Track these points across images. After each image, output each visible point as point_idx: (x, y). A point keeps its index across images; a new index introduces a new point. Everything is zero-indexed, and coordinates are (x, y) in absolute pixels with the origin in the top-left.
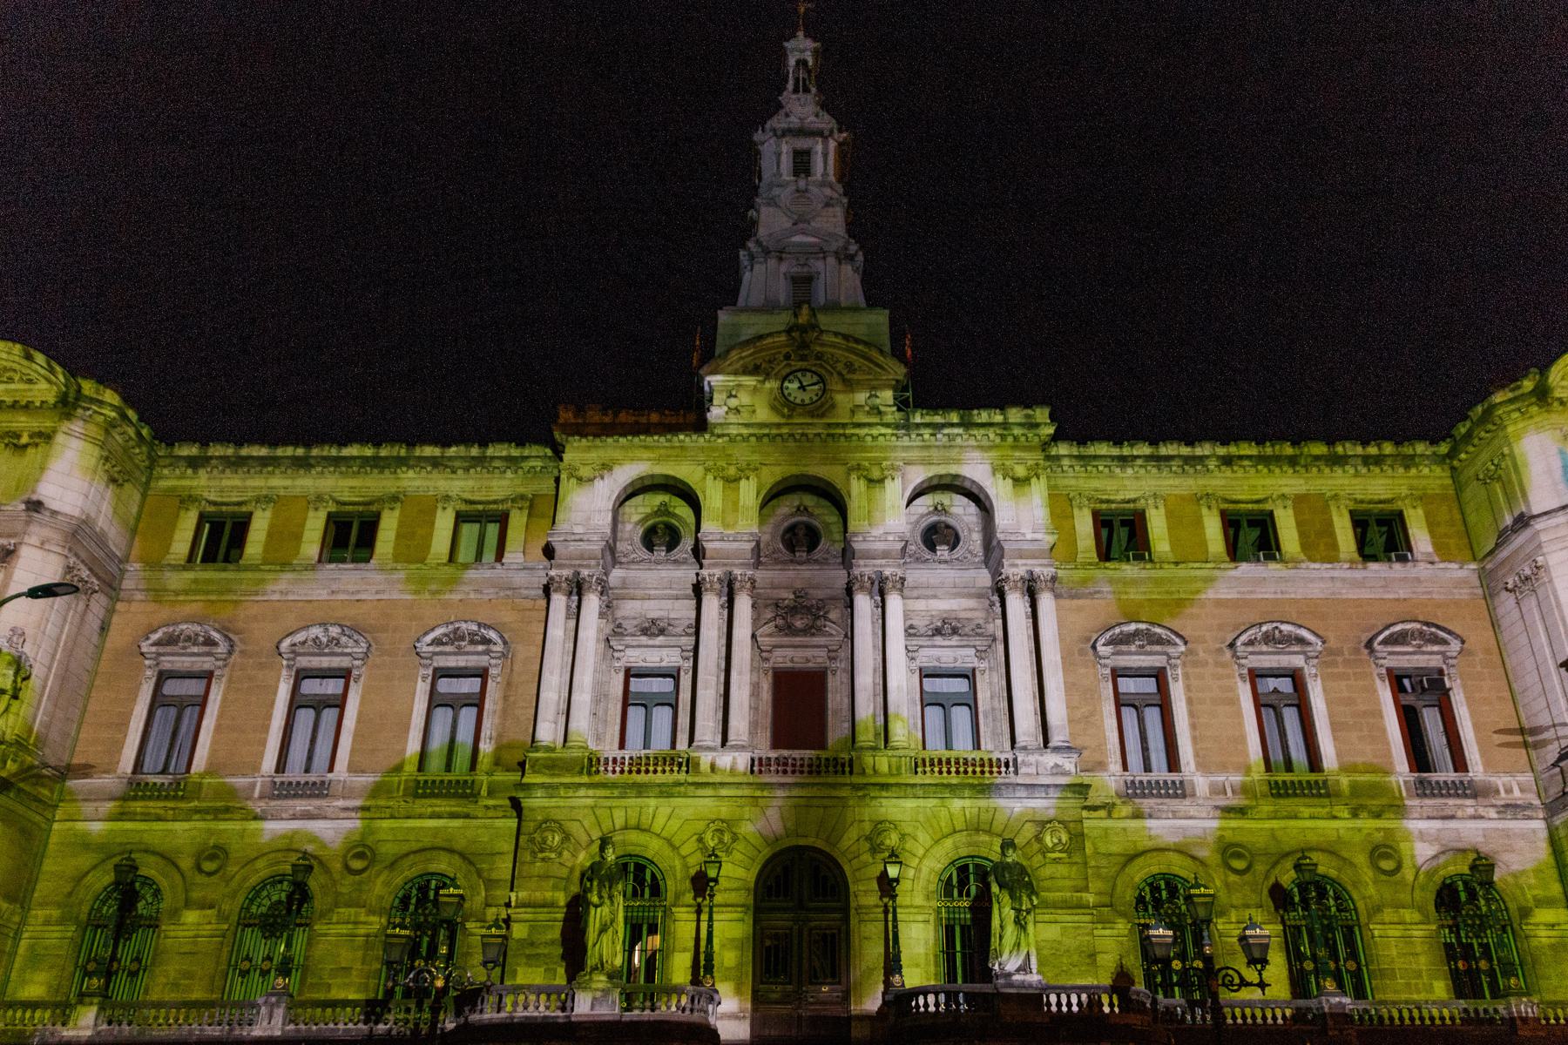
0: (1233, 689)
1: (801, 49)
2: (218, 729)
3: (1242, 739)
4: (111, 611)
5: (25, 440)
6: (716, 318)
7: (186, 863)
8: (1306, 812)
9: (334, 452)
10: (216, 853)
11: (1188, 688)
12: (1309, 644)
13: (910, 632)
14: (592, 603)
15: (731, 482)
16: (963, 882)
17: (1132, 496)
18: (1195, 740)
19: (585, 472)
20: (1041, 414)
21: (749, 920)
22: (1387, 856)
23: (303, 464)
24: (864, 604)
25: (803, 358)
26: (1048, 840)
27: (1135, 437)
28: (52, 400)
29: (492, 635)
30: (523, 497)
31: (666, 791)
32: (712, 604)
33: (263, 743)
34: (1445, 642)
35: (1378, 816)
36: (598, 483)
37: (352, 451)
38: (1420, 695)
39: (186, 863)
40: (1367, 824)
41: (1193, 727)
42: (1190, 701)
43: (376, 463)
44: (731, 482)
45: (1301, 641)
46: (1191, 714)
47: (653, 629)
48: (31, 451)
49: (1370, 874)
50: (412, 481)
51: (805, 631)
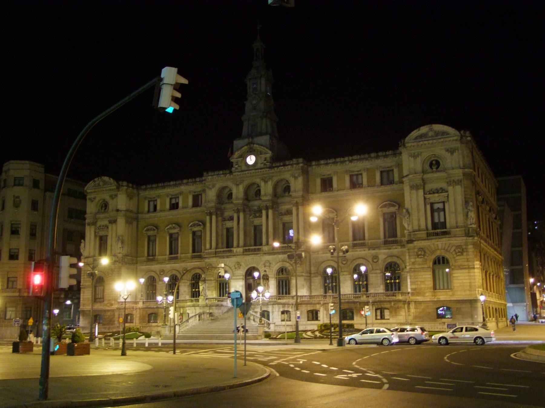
1: (258, 45)
4: (138, 224)
6: (233, 143)
7: (158, 273)
8: (359, 250)
9: (168, 184)
15: (237, 185)
16: (282, 271)
19: (210, 187)
20: (301, 160)
21: (244, 281)
22: (375, 259)
23: (163, 187)
24: (264, 212)
27: (330, 158)
31: (228, 257)
33: (166, 249)
35: (374, 249)
37: (172, 183)
39: (158, 273)
40: (372, 252)
43: (175, 185)
44: (237, 185)
49: (371, 262)
50: (183, 188)
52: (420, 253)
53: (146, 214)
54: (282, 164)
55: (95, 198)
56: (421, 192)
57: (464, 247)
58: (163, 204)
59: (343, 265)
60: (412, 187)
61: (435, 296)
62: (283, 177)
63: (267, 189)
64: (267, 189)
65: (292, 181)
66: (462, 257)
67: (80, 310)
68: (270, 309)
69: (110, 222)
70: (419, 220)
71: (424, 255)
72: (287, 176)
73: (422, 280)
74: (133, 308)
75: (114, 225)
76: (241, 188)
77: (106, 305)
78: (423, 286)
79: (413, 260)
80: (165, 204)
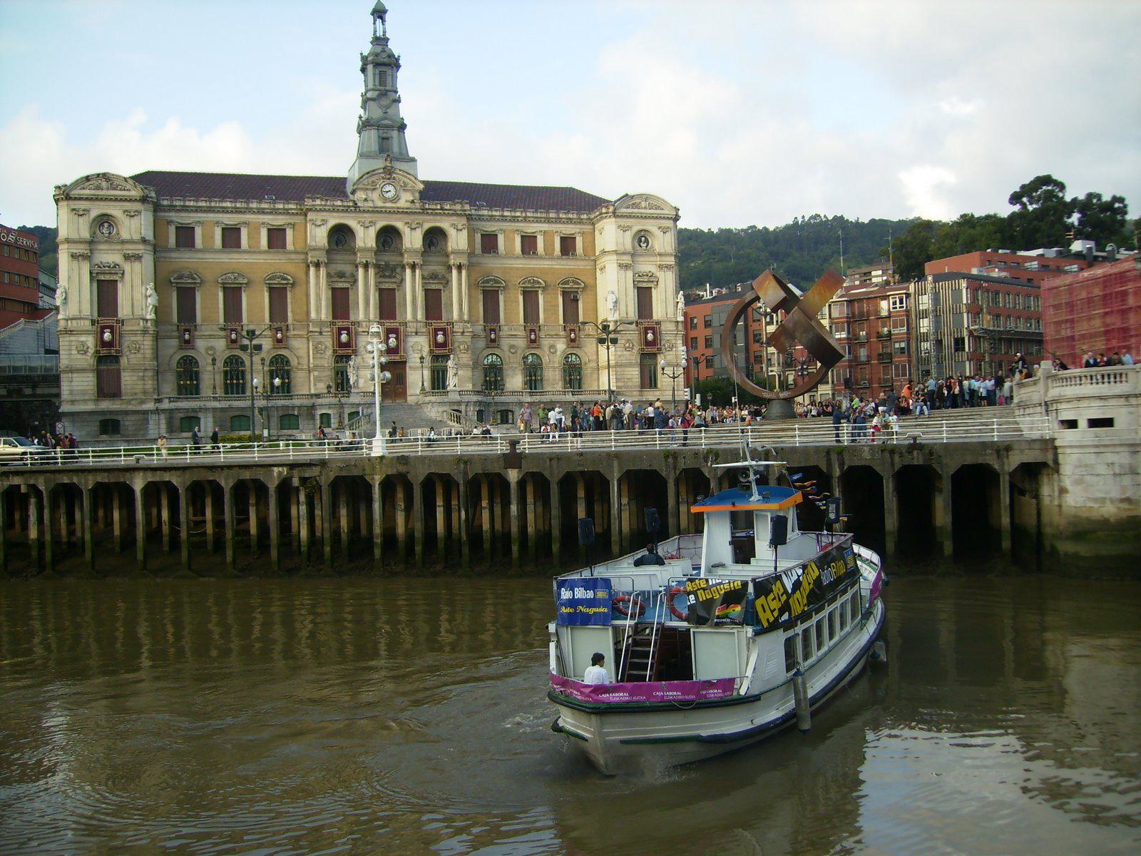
0: (518, 297)
2: (202, 308)
3: (518, 313)
5: (132, 214)
10: (212, 348)
11: (505, 297)
12: (540, 283)
13: (423, 278)
14: (323, 271)
17: (493, 229)
18: (505, 314)
24: (408, 271)
25: (389, 179)
26: (462, 347)
28: (138, 198)
29: (289, 277)
30: (290, 224)
32: (361, 271)
34: (579, 284)
36: (322, 227)
38: (571, 300)
41: (505, 309)
42: (505, 301)
45: (539, 283)
46: (505, 305)
47: (341, 275)
48: (135, 217)
51: (390, 277)
52: (627, 345)
53: (172, 250)
54: (439, 207)
55: (87, 211)
56: (630, 274)
57: (674, 342)
58: (208, 237)
59: (511, 355)
60: (620, 266)
61: (641, 395)
62: (438, 224)
63: (413, 239)
64: (413, 239)
65: (452, 232)
66: (671, 353)
67: (60, 411)
68: (463, 408)
69: (127, 258)
70: (627, 305)
71: (632, 349)
72: (445, 224)
73: (629, 376)
74: (200, 409)
75: (137, 265)
76: (372, 232)
77: (129, 402)
78: (630, 384)
79: (619, 353)
80: (213, 237)
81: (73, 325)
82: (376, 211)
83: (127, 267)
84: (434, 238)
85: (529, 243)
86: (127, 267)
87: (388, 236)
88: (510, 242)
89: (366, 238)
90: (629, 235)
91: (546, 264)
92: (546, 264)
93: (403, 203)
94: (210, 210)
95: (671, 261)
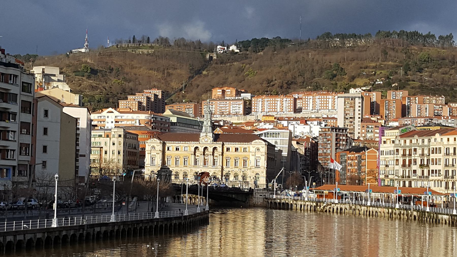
64: (211, 150)
81: (147, 165)
82: (203, 143)
83: (157, 155)
84: (215, 148)
85: (236, 149)
86: (157, 155)
87: (205, 148)
88: (232, 149)
89: (201, 149)
90: (255, 148)
91: (240, 154)
92: (240, 154)
93: (209, 142)
94: (174, 143)
95: (264, 154)
